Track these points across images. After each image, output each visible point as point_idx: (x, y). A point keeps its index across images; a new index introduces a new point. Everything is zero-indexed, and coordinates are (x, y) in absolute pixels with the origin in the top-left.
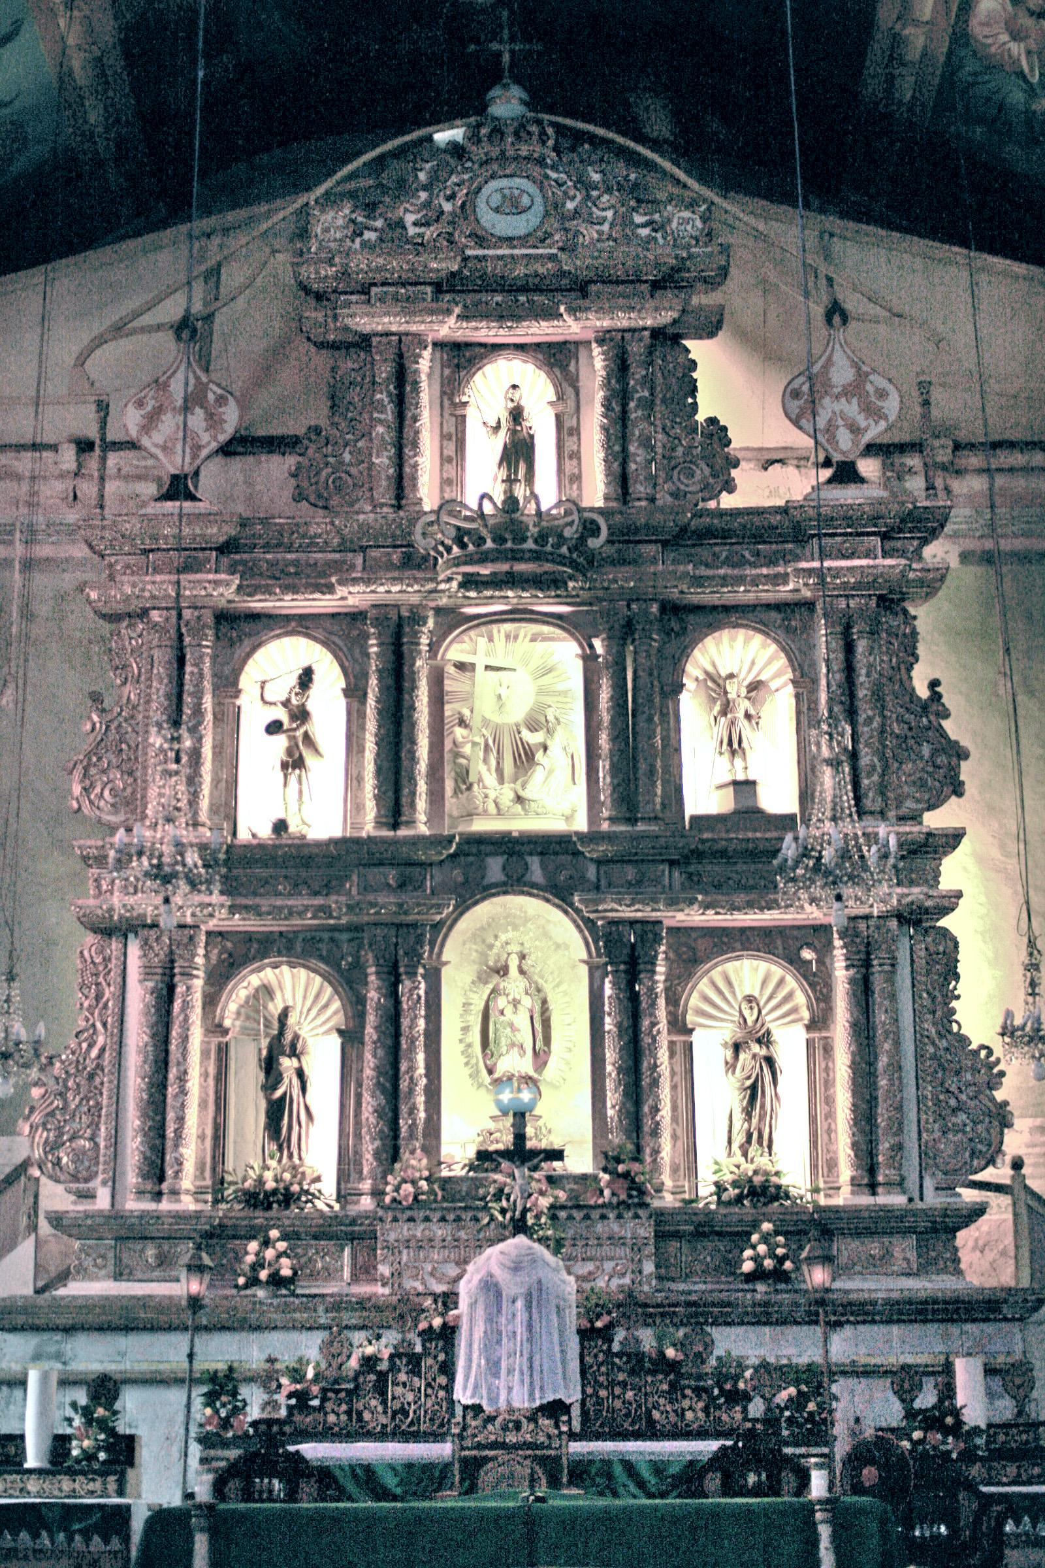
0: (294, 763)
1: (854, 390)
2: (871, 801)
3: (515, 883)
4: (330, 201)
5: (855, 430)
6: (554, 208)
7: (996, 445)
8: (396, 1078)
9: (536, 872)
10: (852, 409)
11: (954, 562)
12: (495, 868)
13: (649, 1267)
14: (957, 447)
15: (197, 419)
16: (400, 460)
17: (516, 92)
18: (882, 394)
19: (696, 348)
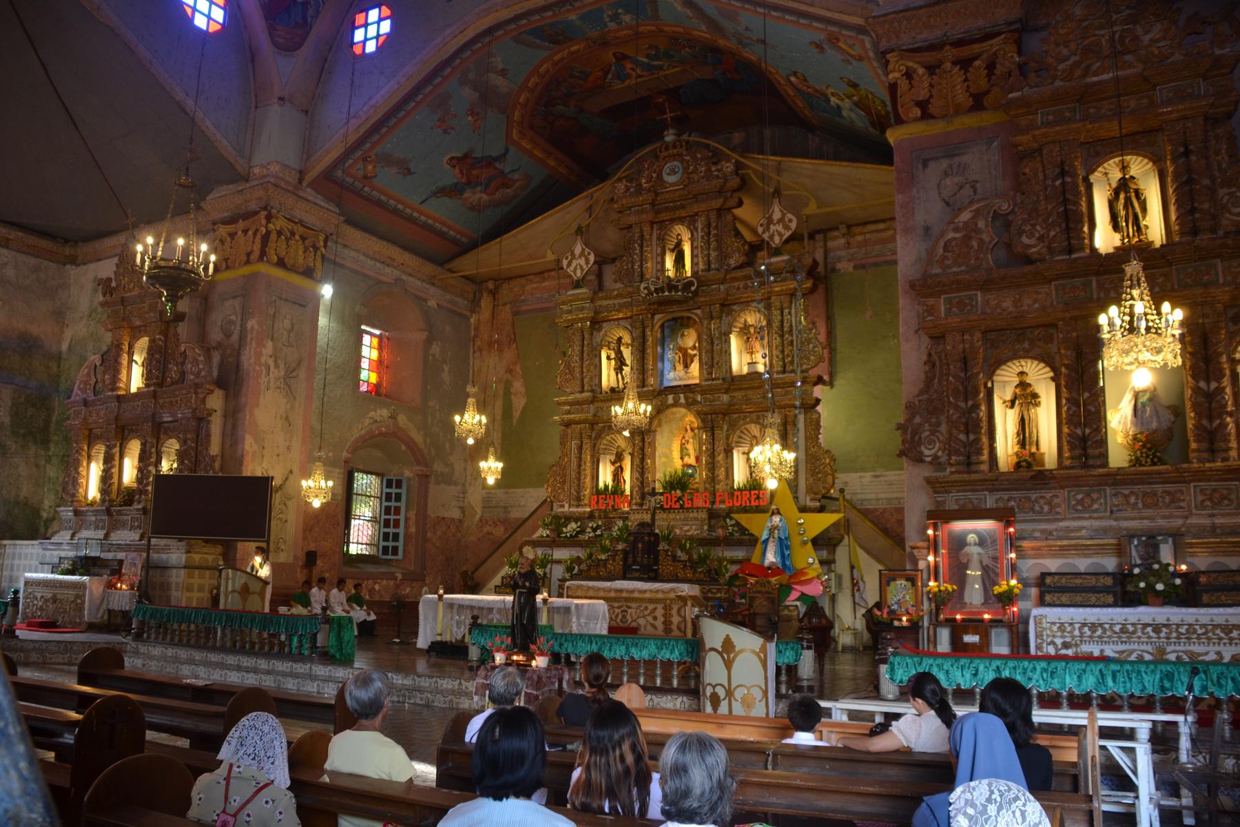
0: (619, 369)
1: (781, 220)
2: (789, 368)
3: (676, 404)
4: (620, 180)
5: (780, 235)
6: (685, 170)
7: (865, 224)
8: (643, 468)
9: (682, 400)
10: (780, 228)
11: (851, 270)
12: (670, 399)
13: (706, 527)
14: (849, 227)
15: (582, 261)
16: (641, 266)
17: (671, 131)
18: (790, 221)
19: (737, 212)
